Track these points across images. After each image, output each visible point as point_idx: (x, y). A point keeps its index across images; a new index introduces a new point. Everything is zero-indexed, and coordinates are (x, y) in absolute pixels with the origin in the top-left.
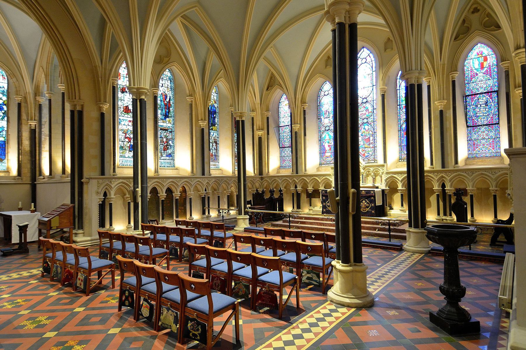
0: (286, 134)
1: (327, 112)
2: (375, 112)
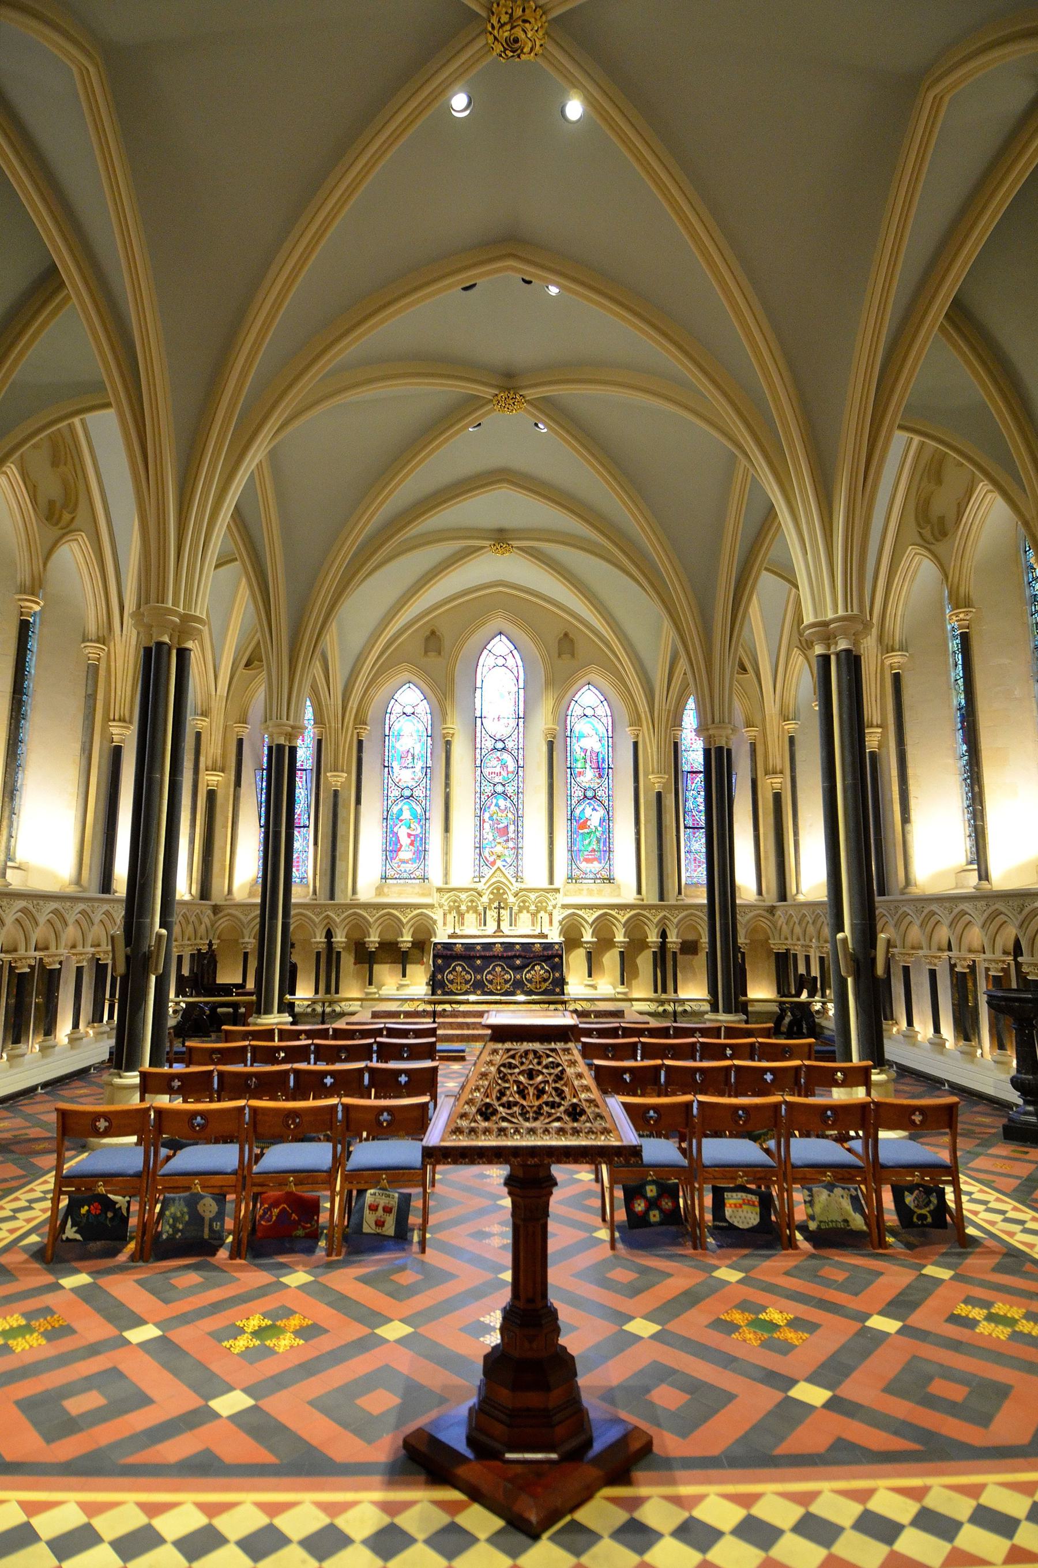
1: (410, 754)
2: (521, 773)
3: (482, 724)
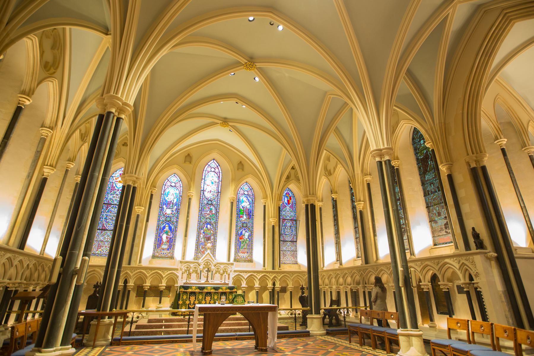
0: (111, 214)
3: (203, 193)
